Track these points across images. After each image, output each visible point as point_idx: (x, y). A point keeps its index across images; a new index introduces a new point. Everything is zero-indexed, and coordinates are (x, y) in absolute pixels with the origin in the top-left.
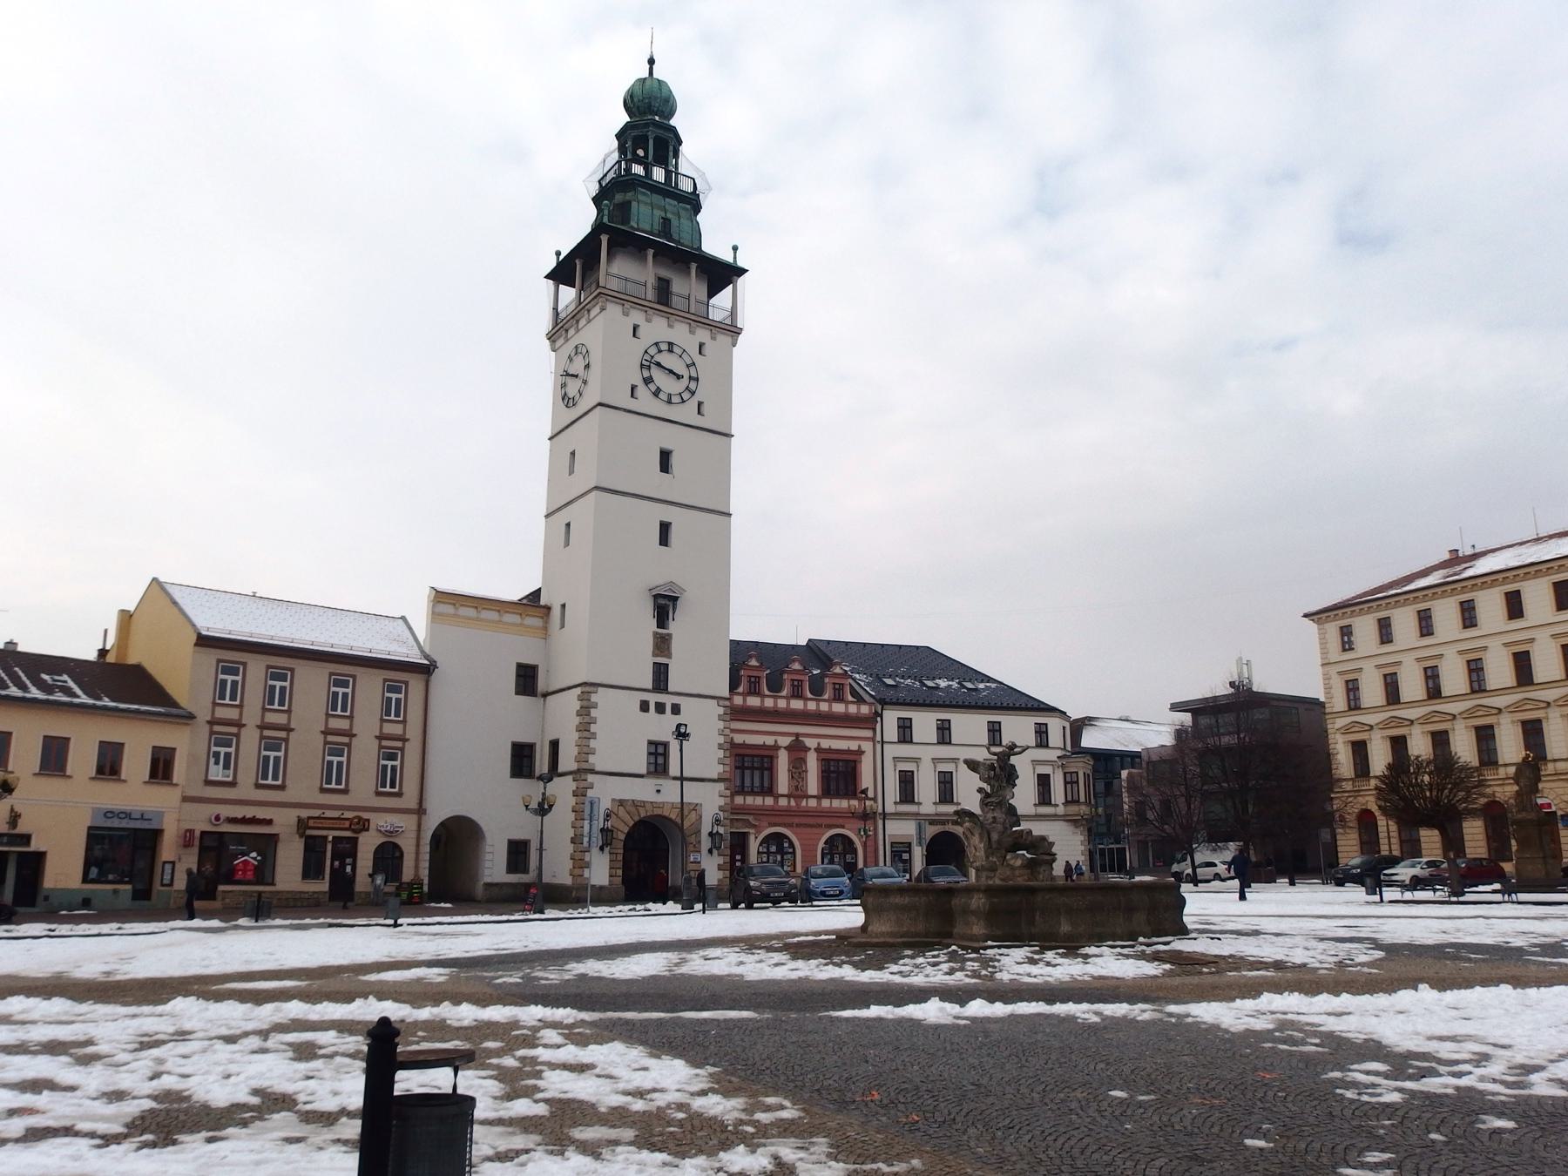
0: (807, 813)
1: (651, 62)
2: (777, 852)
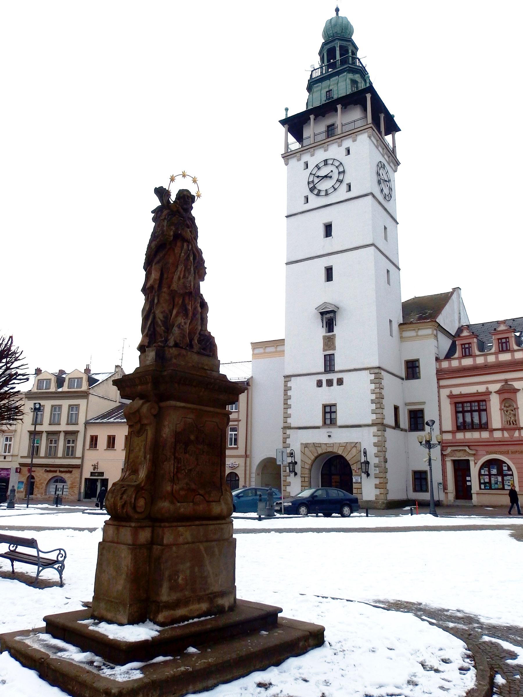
1: (337, 10)
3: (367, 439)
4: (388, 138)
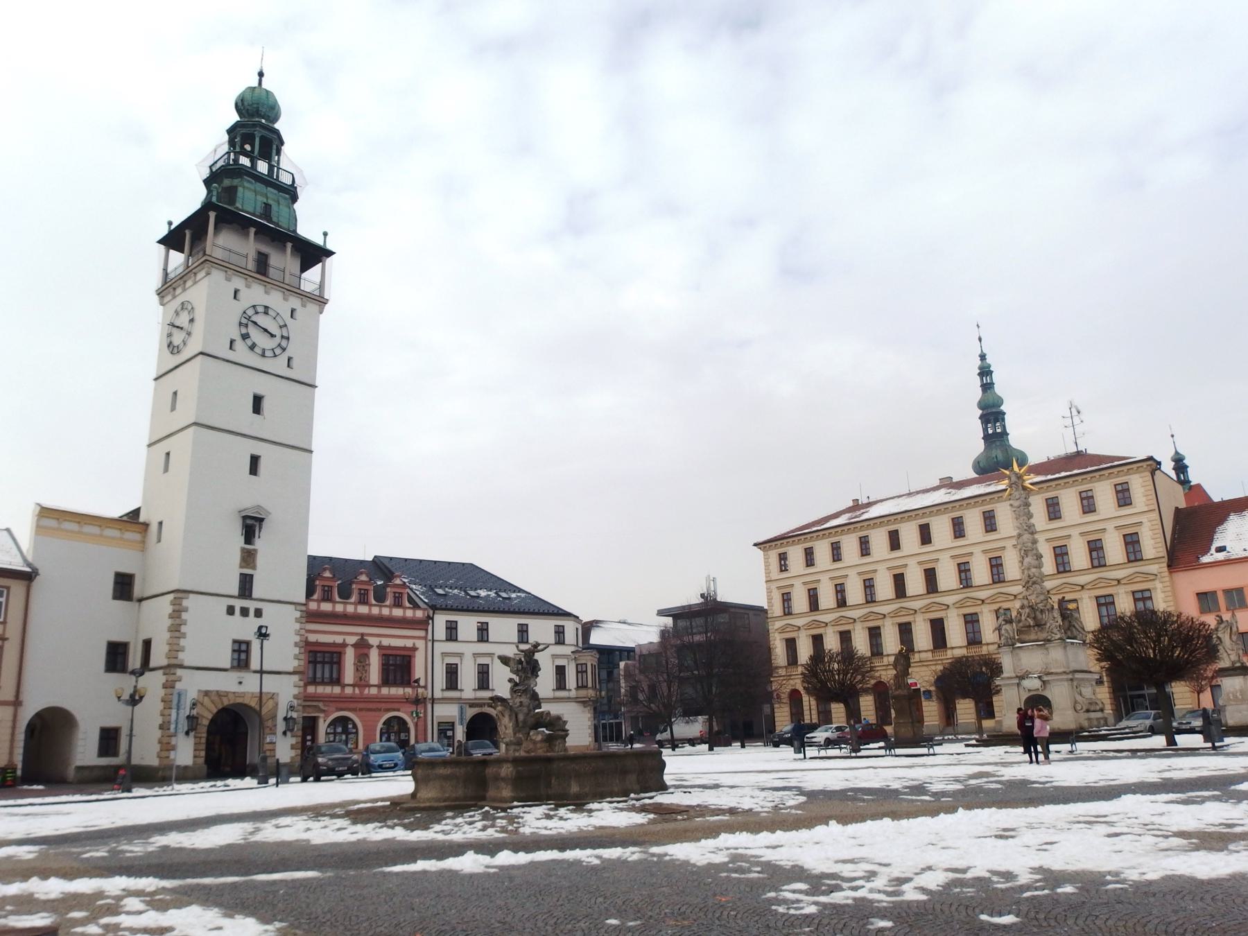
0: (370, 700)
1: (261, 74)
2: (343, 732)
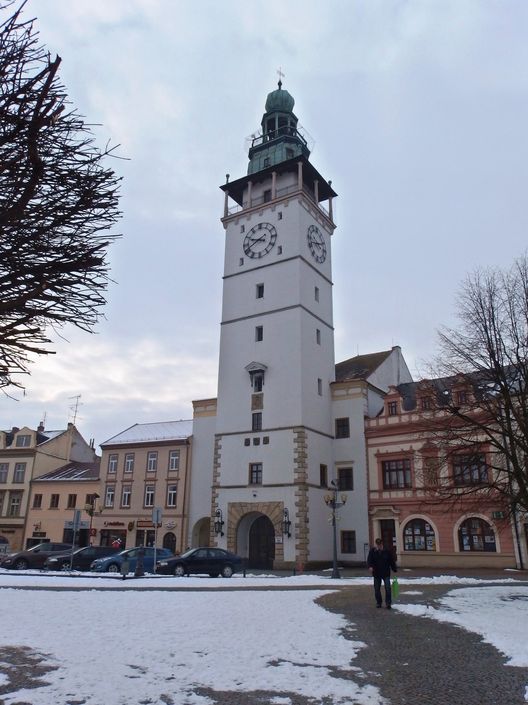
1: (280, 84)
2: (421, 535)
3: (289, 499)
4: (324, 205)
